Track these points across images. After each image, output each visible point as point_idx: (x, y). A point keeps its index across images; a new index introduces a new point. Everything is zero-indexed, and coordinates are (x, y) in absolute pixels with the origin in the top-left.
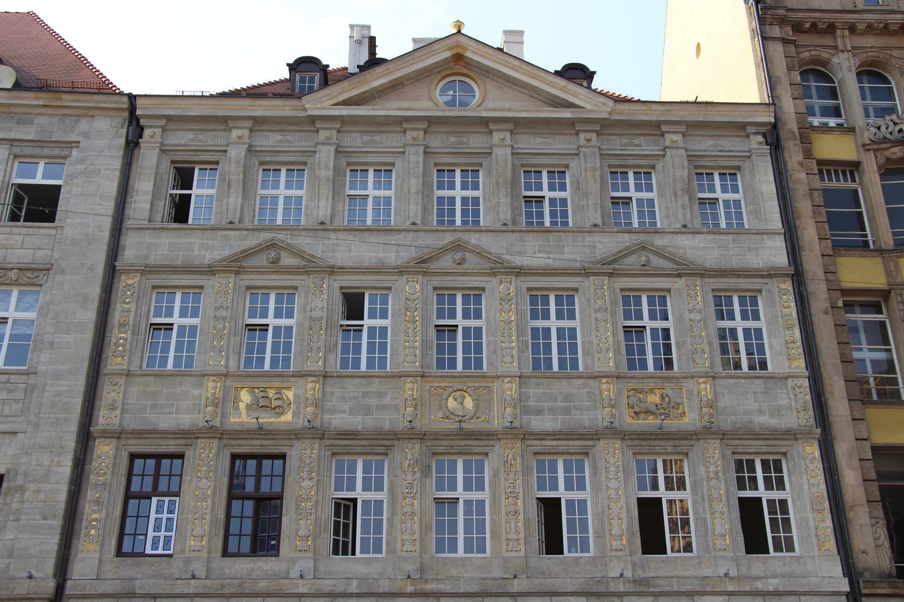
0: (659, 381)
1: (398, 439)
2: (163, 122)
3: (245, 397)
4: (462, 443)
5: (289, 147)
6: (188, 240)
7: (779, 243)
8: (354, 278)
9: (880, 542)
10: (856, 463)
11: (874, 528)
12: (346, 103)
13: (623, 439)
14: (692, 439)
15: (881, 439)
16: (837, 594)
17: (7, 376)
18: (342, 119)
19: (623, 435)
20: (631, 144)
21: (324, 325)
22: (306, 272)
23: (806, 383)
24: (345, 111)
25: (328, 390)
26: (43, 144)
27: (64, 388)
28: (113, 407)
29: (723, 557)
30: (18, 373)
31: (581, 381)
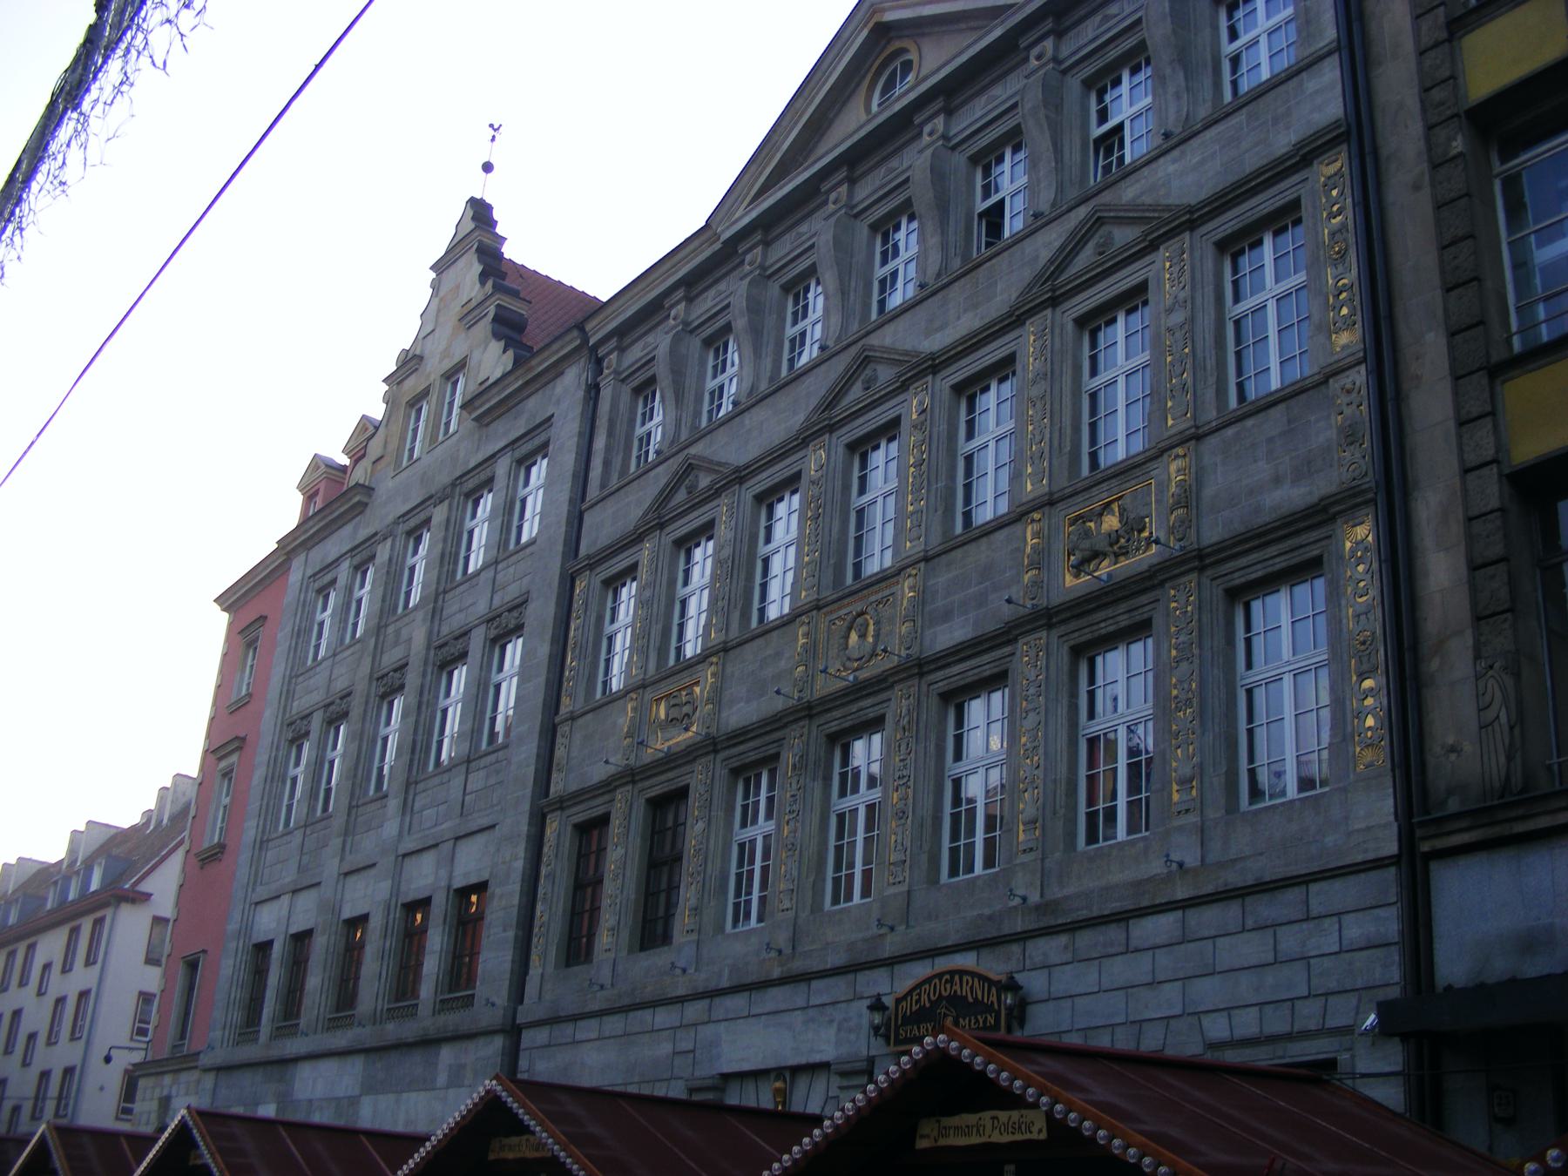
0: (1114, 482)
1: (785, 726)
4: (854, 708)
7: (1330, 74)
9: (1490, 715)
10: (1456, 529)
11: (1481, 683)
13: (1050, 626)
14: (1153, 588)
15: (1528, 449)
16: (1377, 864)
19: (1047, 618)
20: (1107, 18)
23: (1359, 376)
25: (729, 670)
29: (1181, 829)
31: (1005, 532)
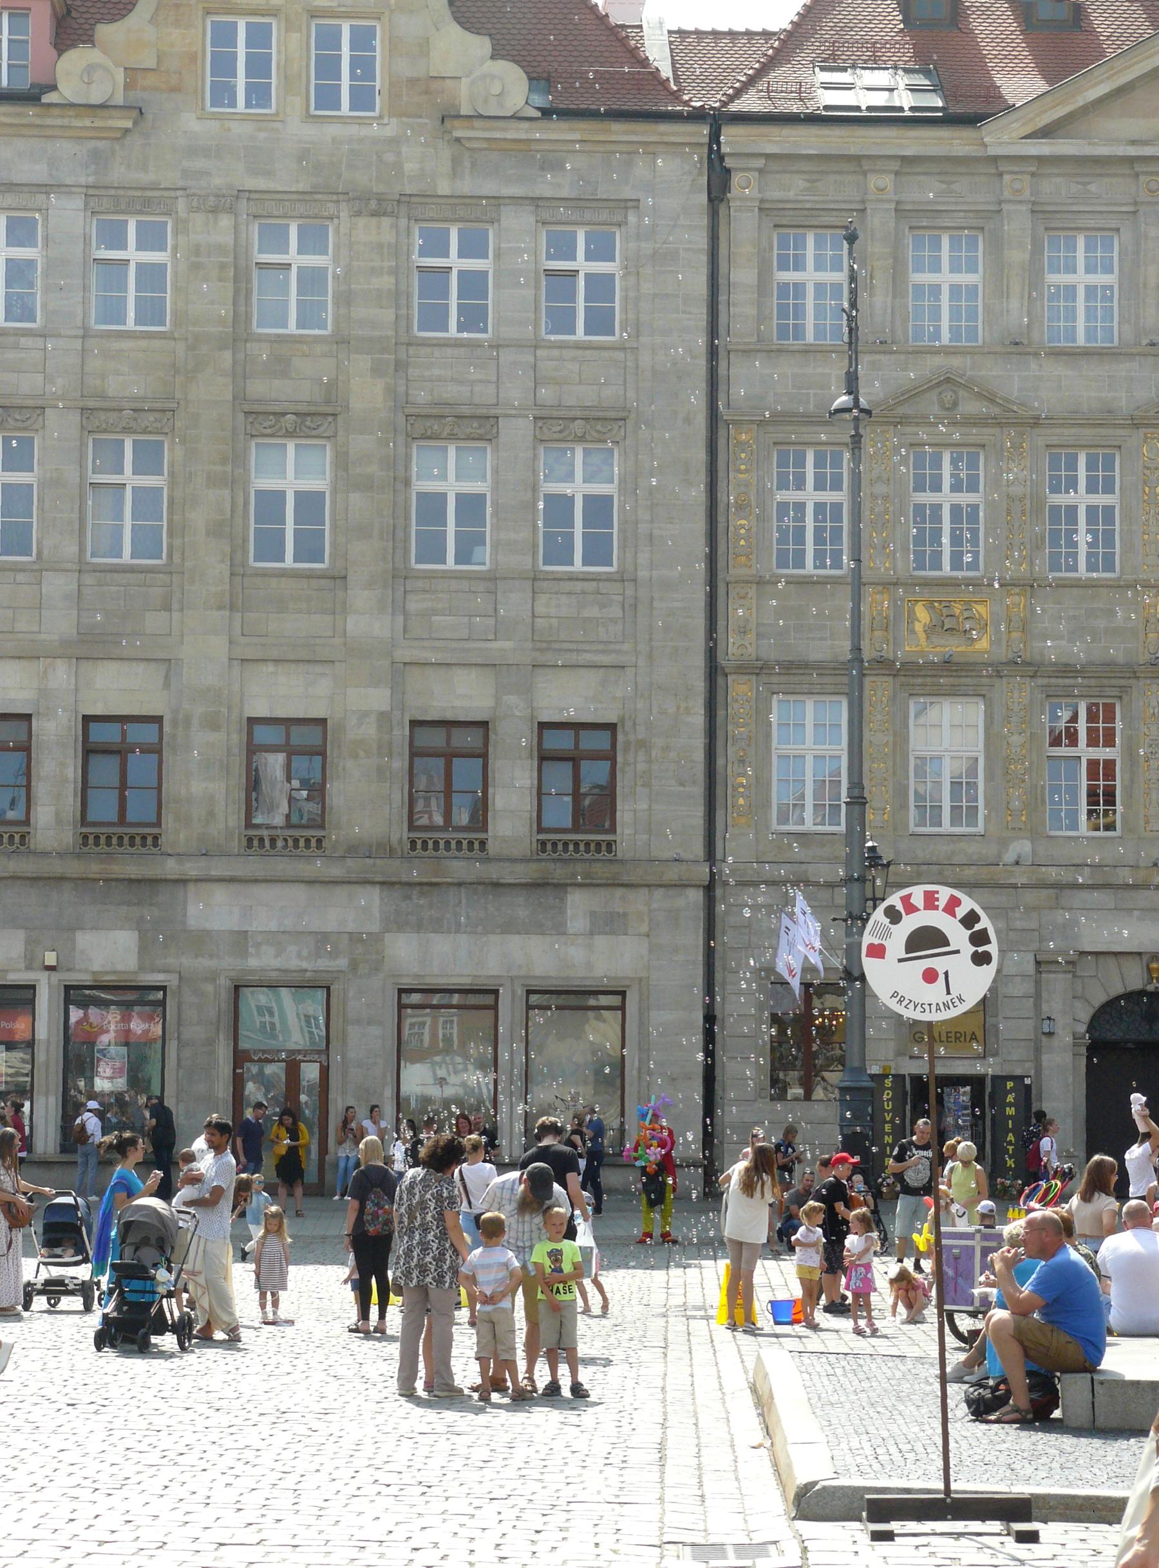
2: (761, 163)
3: (923, 615)
5: (957, 203)
6: (820, 370)
8: (1066, 431)
12: (1046, 132)
17: (594, 584)
18: (1041, 160)
21: (1028, 506)
22: (998, 423)
24: (1043, 148)
26: (583, 204)
27: (678, 604)
28: (743, 631)
30: (609, 578)
